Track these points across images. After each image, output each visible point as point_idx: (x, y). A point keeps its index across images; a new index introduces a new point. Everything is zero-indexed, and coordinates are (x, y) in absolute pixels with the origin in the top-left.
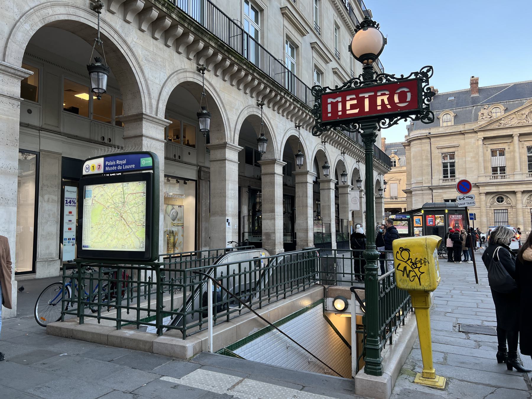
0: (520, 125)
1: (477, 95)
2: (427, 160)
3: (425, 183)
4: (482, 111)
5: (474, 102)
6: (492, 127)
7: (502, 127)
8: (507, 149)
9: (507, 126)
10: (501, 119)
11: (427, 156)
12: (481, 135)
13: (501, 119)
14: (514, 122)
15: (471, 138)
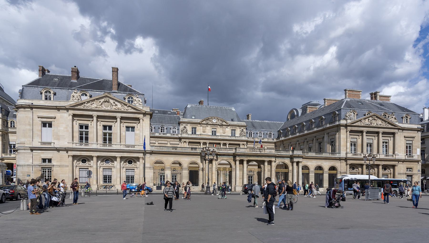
0: (97, 109)
1: (75, 81)
2: (30, 125)
3: (27, 144)
4: (74, 94)
5: (71, 86)
6: (79, 107)
7: (85, 108)
8: (89, 125)
9: (89, 108)
10: (85, 103)
11: (29, 122)
12: (71, 112)
13: (85, 103)
14: (94, 106)
15: (64, 113)
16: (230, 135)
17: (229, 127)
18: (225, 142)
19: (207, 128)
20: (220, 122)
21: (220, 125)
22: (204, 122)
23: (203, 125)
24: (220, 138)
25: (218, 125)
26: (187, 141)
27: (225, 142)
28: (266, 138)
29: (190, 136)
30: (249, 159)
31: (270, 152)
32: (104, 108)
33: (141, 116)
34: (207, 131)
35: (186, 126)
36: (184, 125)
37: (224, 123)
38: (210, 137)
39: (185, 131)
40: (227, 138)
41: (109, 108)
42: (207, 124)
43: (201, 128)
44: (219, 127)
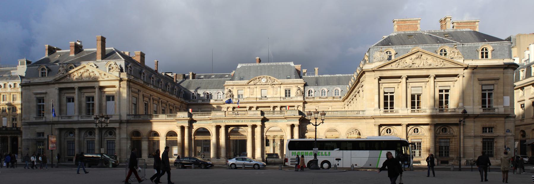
16: (284, 96)
17: (282, 86)
18: (275, 104)
22: (252, 83)
23: (251, 86)
24: (269, 100)
30: (227, 124)
31: (254, 114)
34: (255, 93)
35: (232, 90)
36: (230, 88)
37: (276, 83)
40: (279, 100)
42: (255, 85)
43: (248, 90)
44: (270, 86)
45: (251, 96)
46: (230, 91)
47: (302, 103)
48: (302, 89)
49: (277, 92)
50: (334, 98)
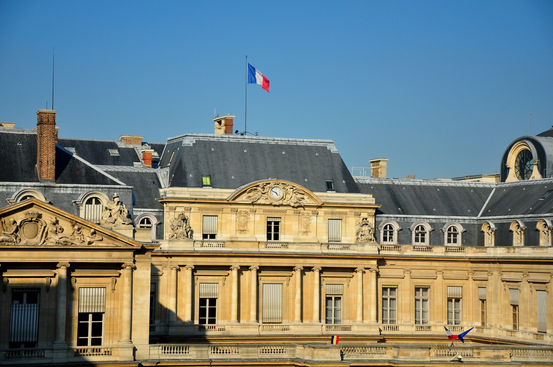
17: (321, 211)
18: (309, 262)
19: (252, 216)
20: (292, 198)
21: (293, 207)
24: (292, 249)
25: (289, 205)
26: (191, 262)
27: (309, 262)
28: (441, 244)
29: (198, 248)
32: (23, 242)
33: (126, 257)
34: (251, 226)
35: (187, 214)
36: (180, 209)
37: (307, 201)
38: (263, 249)
39: (181, 230)
40: (316, 250)
41: (37, 241)
42: (253, 204)
43: (233, 217)
45: (241, 237)
46: (185, 220)
47: (375, 262)
48: (371, 221)
49: (308, 226)
50: (447, 250)
